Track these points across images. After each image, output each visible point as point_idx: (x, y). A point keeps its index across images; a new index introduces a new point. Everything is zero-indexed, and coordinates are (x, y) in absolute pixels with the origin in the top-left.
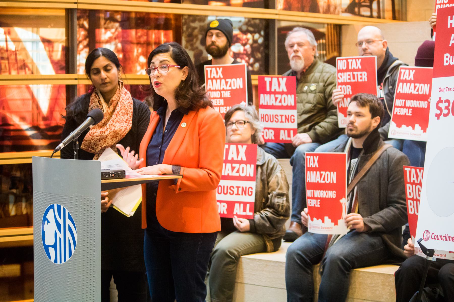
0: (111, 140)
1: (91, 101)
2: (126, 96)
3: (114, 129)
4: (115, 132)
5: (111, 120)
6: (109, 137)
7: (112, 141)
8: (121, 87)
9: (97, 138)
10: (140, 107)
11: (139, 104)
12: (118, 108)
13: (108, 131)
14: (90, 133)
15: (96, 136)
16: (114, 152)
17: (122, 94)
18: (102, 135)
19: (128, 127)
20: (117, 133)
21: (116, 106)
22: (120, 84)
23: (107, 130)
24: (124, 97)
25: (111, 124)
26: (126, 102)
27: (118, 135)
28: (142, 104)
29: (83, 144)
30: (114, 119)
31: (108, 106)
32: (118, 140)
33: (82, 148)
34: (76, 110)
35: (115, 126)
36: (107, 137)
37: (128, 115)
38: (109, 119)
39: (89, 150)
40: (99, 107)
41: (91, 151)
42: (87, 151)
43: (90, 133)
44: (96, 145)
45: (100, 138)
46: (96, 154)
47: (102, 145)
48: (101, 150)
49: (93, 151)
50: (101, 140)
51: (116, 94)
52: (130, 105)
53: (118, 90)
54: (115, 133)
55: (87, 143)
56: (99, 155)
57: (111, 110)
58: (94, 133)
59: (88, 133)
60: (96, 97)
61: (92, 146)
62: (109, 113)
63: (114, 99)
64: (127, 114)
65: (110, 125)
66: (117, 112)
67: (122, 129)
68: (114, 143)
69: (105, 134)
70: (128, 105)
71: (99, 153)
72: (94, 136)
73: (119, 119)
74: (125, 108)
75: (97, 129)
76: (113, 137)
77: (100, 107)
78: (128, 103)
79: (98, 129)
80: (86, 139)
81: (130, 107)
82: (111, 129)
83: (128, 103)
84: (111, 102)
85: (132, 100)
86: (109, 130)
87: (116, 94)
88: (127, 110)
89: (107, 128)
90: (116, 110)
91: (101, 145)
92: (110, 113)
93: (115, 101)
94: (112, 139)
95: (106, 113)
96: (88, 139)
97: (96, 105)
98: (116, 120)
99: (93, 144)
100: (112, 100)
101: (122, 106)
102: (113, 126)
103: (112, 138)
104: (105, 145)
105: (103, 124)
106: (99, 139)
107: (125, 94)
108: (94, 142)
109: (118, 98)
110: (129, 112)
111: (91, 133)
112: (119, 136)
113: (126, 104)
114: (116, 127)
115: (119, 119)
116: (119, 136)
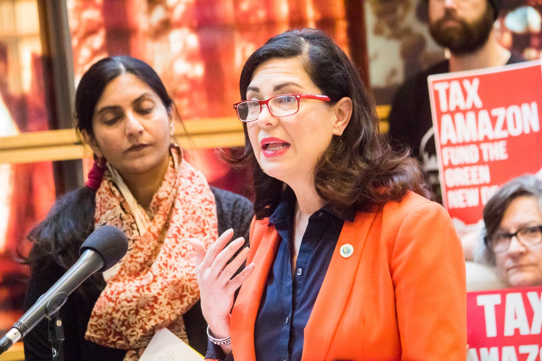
0: (168, 308)
1: (98, 205)
2: (193, 183)
3: (175, 276)
4: (176, 284)
5: (161, 254)
6: (161, 299)
7: (172, 308)
8: (176, 160)
9: (128, 305)
10: (236, 211)
11: (232, 203)
12: (177, 219)
13: (159, 283)
14: (109, 293)
15: (126, 300)
16: (177, 338)
17: (182, 180)
18: (141, 294)
20: (183, 287)
21: (171, 212)
22: (173, 151)
23: (154, 281)
24: (190, 187)
25: (164, 264)
26: (196, 201)
27: (185, 293)
28: (239, 202)
29: (91, 325)
30: (170, 250)
31: (149, 216)
32: (186, 304)
33: (89, 337)
34: (59, 235)
35: (175, 269)
36: (155, 299)
37: (205, 235)
38: (155, 250)
39: (108, 339)
40: (125, 219)
41: (114, 343)
42: (103, 343)
43: (109, 293)
44: (129, 323)
45: (137, 306)
46: (131, 349)
47: (146, 324)
48: (142, 336)
49: (121, 342)
51: (164, 179)
52: (208, 207)
53: (170, 168)
54: (177, 288)
55: (101, 321)
56: (138, 352)
57: (160, 226)
58: (119, 293)
59: (103, 294)
60: (112, 193)
61: (118, 330)
62: (154, 235)
63: (161, 194)
64: (203, 231)
65: (160, 267)
66: (177, 229)
67: (194, 275)
68: (178, 316)
69: (150, 292)
70: (204, 206)
71: (137, 346)
72: (120, 300)
73: (183, 248)
74: (196, 216)
75: (126, 282)
76: (176, 299)
77: (128, 220)
78: (203, 201)
79: (129, 280)
80: (98, 312)
81: (208, 213)
82: (166, 278)
83: (203, 201)
84: (154, 203)
85: (211, 194)
86: (160, 280)
87: (164, 179)
88: (201, 220)
89: (155, 277)
90: (171, 224)
91: (141, 323)
92: (157, 234)
93: (167, 198)
94: (171, 304)
95: (145, 236)
96: (105, 311)
97: (116, 215)
98: (176, 250)
99: (121, 323)
100: (157, 197)
101: (187, 213)
102: (171, 267)
103: (171, 302)
104: (152, 323)
105: (141, 264)
106: (135, 308)
107: (190, 178)
108: (123, 317)
109: (174, 190)
110: (207, 227)
111: (112, 293)
112: (188, 294)
113: (198, 206)
114: (179, 269)
115: (183, 248)
116: (188, 294)
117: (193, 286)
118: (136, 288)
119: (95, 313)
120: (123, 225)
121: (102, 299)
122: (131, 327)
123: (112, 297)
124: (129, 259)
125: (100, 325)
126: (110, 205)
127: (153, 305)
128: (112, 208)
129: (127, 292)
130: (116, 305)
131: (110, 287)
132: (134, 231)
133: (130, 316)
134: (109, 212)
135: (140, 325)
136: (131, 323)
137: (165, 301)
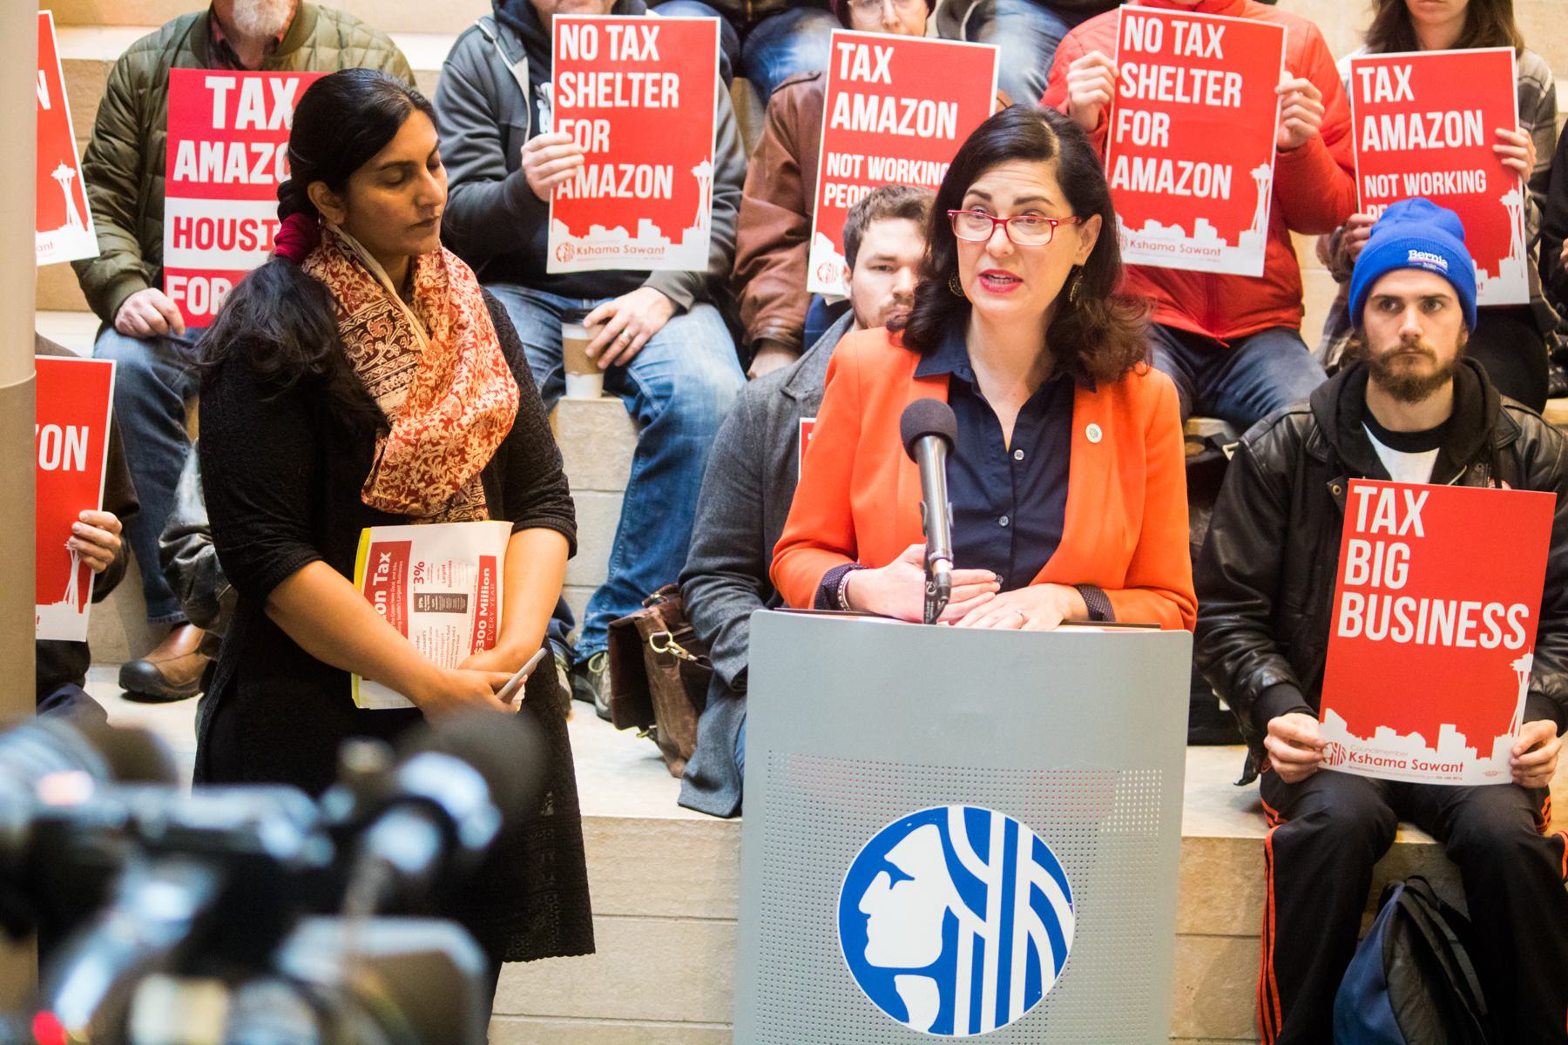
3: (485, 406)
15: (430, 442)
18: (451, 434)
19: (510, 389)
27: (494, 429)
29: (381, 481)
32: (494, 447)
37: (490, 344)
41: (405, 506)
43: (401, 434)
44: (431, 477)
47: (456, 477)
49: (415, 505)
50: (450, 458)
61: (413, 487)
62: (443, 345)
64: (487, 337)
67: (502, 402)
79: (422, 414)
80: (392, 462)
84: (419, 295)
86: (468, 410)
89: (463, 407)
95: (432, 347)
96: (400, 459)
99: (419, 476)
100: (421, 285)
105: (433, 389)
108: (423, 468)
117: (502, 418)
118: (442, 424)
119: (386, 462)
120: (394, 328)
121: (393, 442)
122: (435, 483)
123: (408, 437)
124: (416, 382)
125: (393, 481)
126: (367, 295)
127: (463, 449)
128: (372, 301)
129: (431, 429)
130: (416, 450)
131: (400, 426)
132: (412, 338)
133: (433, 466)
134: (366, 305)
135: (447, 479)
136: (434, 476)
137: (476, 444)
